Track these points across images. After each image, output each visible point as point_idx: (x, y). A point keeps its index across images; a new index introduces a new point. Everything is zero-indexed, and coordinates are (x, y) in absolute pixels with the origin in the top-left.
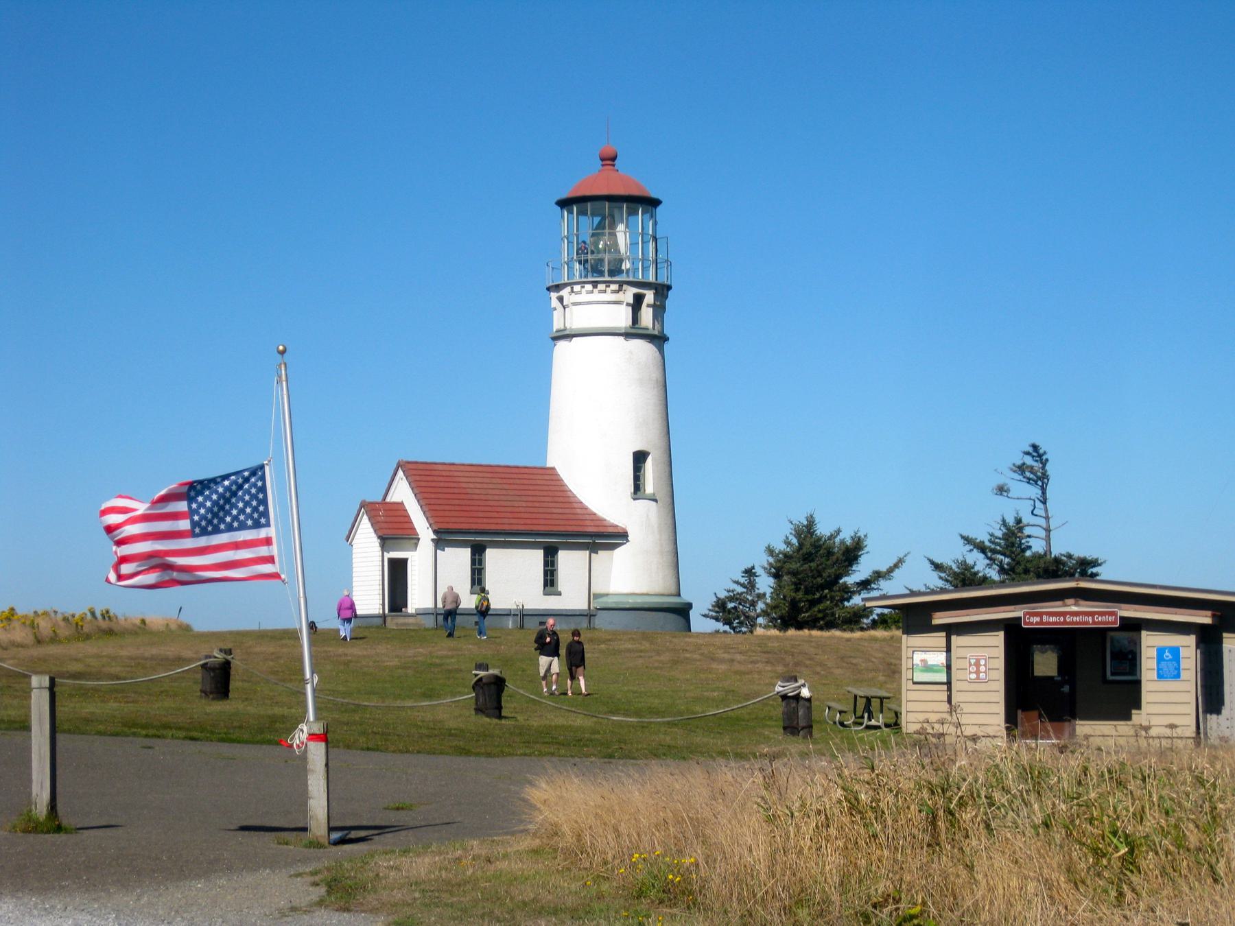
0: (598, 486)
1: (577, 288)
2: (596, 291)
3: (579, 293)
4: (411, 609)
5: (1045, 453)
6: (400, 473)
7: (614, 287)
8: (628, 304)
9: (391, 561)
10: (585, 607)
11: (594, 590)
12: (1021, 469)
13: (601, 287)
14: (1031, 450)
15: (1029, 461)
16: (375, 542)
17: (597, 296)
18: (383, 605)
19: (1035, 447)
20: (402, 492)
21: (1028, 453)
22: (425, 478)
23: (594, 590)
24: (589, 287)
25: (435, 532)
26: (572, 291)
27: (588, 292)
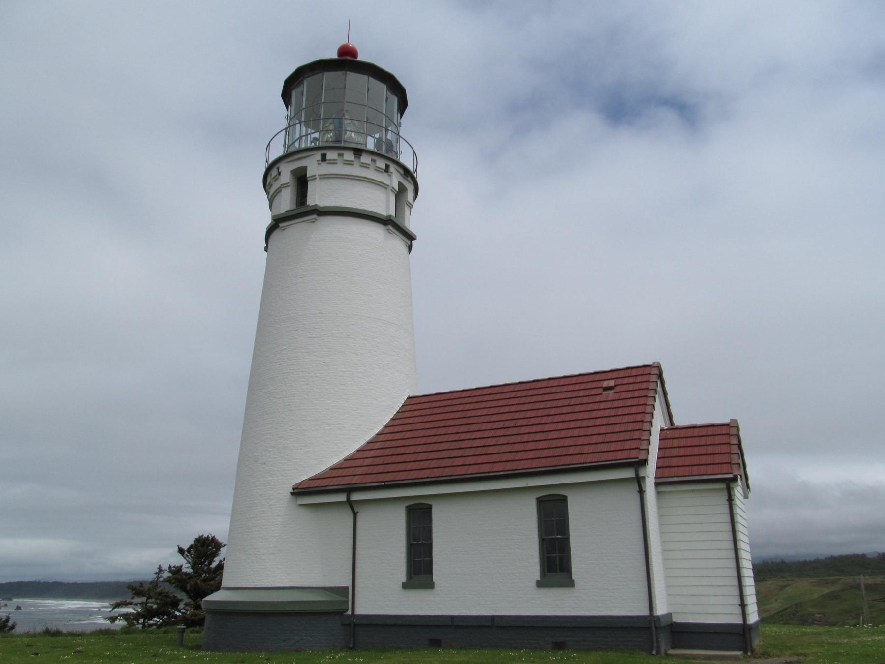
1: (331, 155)
3: (333, 162)
7: (381, 164)
8: (393, 190)
13: (366, 159)
17: (356, 170)
24: (349, 156)
26: (324, 158)
27: (349, 163)
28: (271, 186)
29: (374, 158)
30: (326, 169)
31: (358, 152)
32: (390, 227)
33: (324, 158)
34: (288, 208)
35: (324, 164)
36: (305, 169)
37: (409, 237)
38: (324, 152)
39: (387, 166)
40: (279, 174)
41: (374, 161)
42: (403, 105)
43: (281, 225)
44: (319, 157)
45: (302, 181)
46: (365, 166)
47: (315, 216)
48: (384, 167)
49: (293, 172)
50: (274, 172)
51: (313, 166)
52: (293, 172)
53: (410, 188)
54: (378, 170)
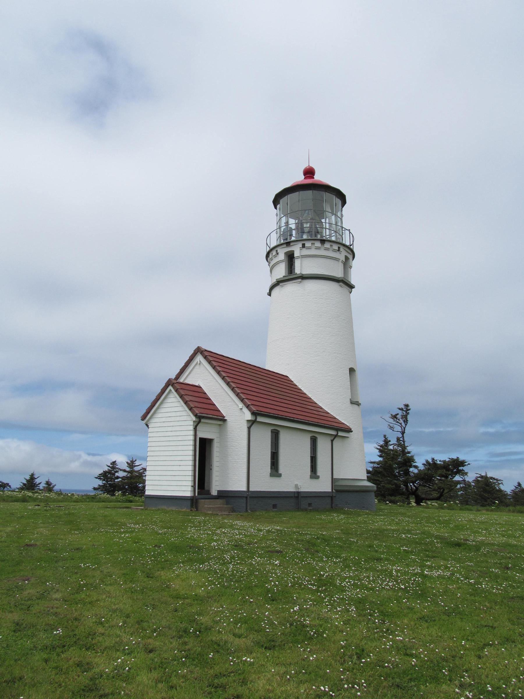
0: (324, 391)
1: (308, 244)
2: (323, 248)
3: (309, 248)
4: (214, 493)
5: (410, 409)
6: (199, 358)
7: (336, 247)
9: (201, 439)
10: (330, 490)
11: (335, 477)
12: (395, 417)
13: (327, 245)
14: (403, 407)
15: (400, 412)
16: (189, 419)
18: (194, 486)
19: (407, 406)
20: (203, 377)
21: (401, 409)
22: (223, 365)
23: (335, 477)
24: (318, 244)
25: (253, 413)
26: (304, 246)
27: (318, 248)
28: (272, 259)
29: (331, 244)
30: (305, 252)
31: (323, 241)
32: (341, 284)
33: (304, 246)
34: (284, 275)
35: (304, 249)
36: (293, 251)
37: (351, 287)
38: (303, 242)
39: (339, 248)
40: (278, 254)
41: (331, 246)
42: (344, 202)
43: (281, 284)
44: (300, 245)
45: (290, 258)
46: (327, 249)
47: (300, 280)
48: (337, 249)
49: (286, 253)
50: (274, 253)
51: (297, 250)
52: (286, 253)
53: (350, 257)
54: (334, 251)
